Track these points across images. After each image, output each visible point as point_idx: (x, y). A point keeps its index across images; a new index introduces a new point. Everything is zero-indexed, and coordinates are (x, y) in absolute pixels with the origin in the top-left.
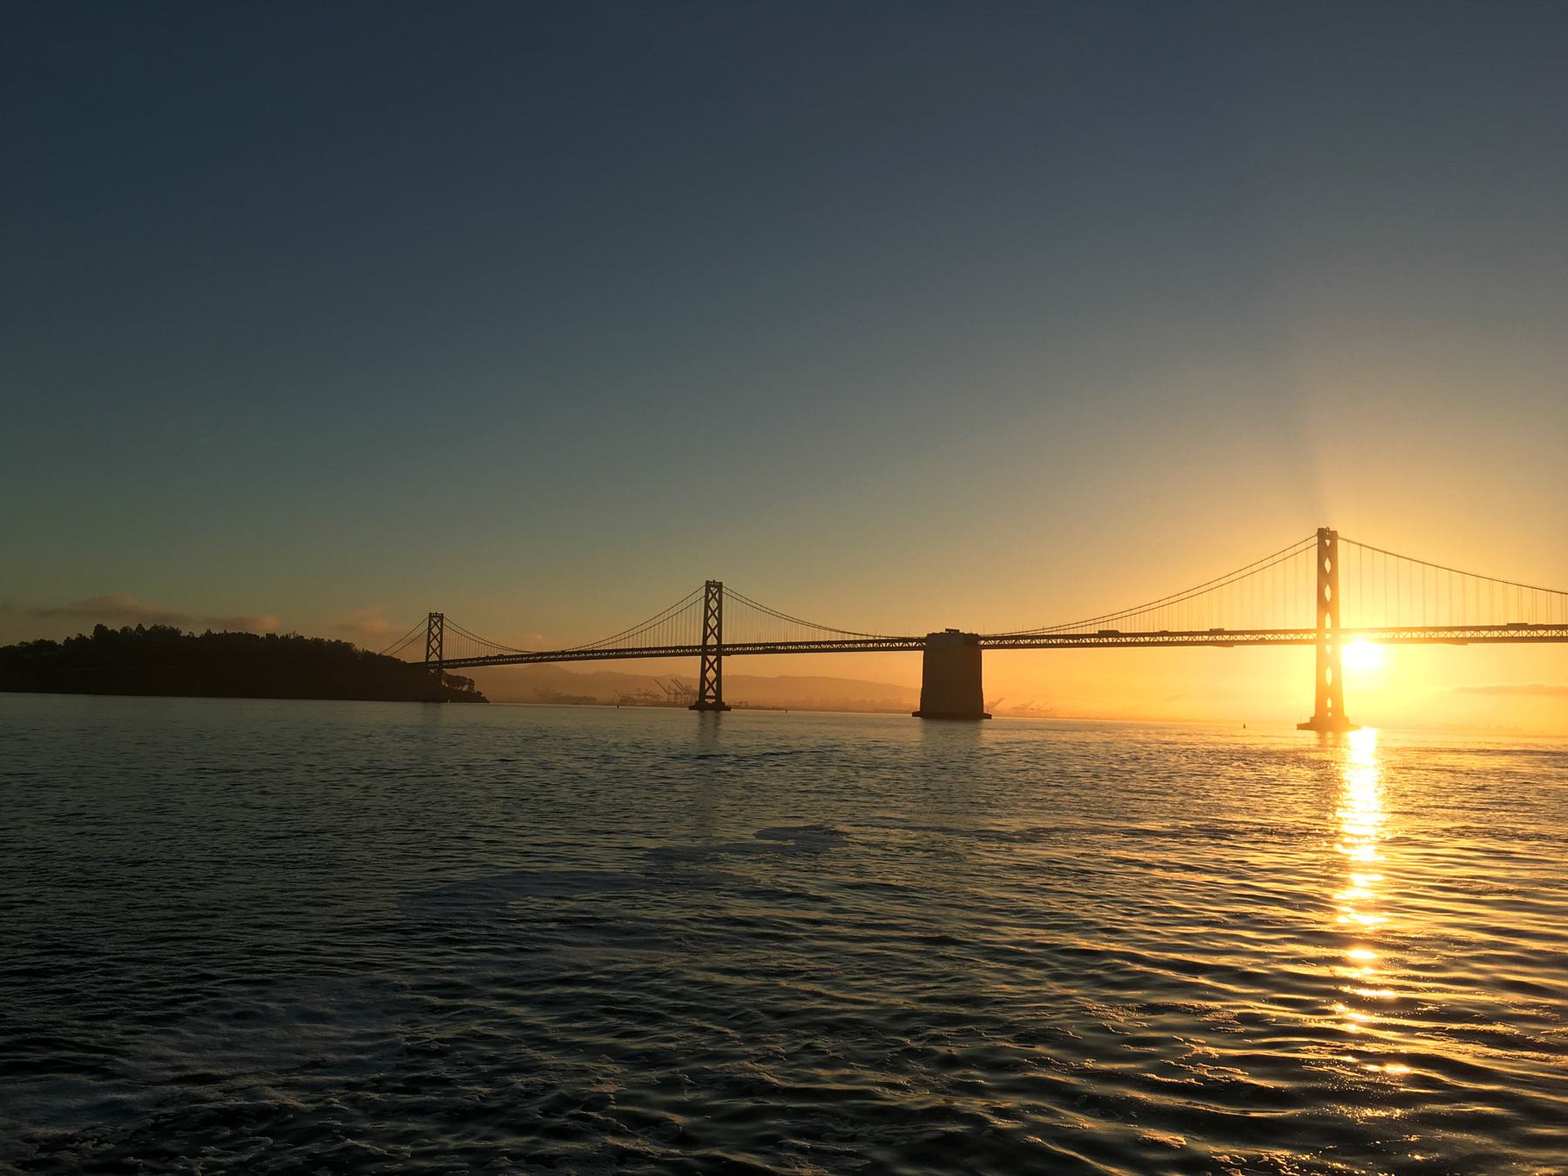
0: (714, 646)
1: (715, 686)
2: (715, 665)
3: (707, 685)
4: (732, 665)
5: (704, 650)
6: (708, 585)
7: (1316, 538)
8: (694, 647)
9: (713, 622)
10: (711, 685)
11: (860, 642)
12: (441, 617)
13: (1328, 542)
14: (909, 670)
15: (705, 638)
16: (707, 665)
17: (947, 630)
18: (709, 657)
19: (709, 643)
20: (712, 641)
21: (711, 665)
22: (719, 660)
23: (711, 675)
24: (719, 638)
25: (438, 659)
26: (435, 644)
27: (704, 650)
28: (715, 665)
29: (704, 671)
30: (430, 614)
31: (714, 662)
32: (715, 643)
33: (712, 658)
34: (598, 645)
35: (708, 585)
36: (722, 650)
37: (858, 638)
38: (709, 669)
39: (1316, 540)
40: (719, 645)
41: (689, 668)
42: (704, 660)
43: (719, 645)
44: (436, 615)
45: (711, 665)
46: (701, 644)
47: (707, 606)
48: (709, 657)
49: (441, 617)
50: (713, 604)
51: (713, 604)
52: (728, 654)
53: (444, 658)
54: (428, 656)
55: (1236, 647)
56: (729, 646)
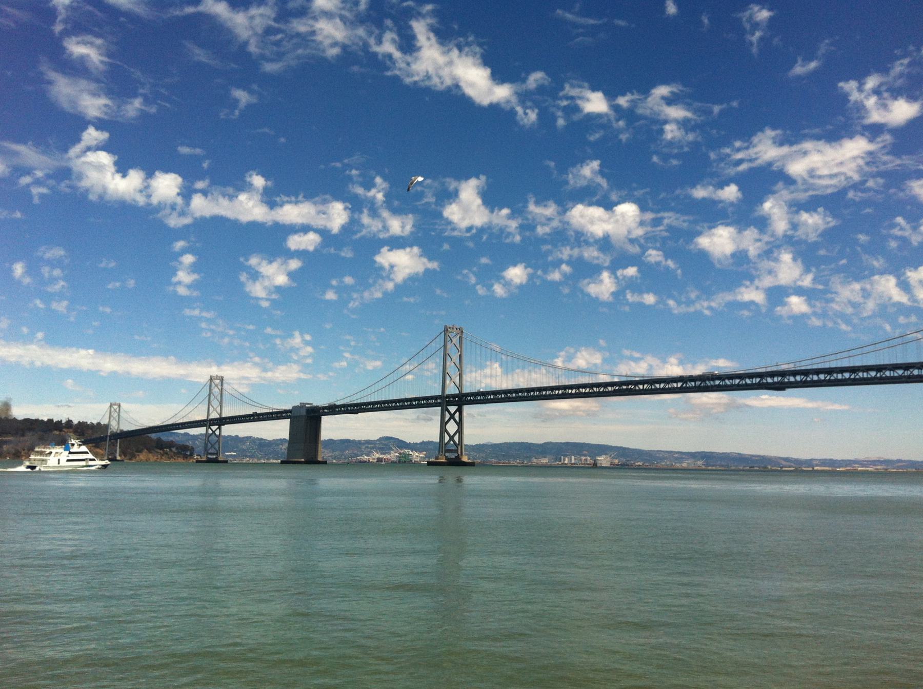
0: (454, 396)
2: (457, 416)
8: (435, 398)
10: (452, 438)
16: (447, 416)
18: (448, 407)
19: (448, 392)
20: (451, 390)
22: (460, 410)
23: (452, 427)
25: (217, 416)
26: (215, 403)
28: (457, 416)
30: (211, 377)
31: (455, 413)
33: (453, 409)
35: (446, 330)
36: (462, 400)
44: (217, 377)
45: (452, 416)
47: (445, 355)
48: (448, 407)
53: (225, 414)
54: (208, 415)
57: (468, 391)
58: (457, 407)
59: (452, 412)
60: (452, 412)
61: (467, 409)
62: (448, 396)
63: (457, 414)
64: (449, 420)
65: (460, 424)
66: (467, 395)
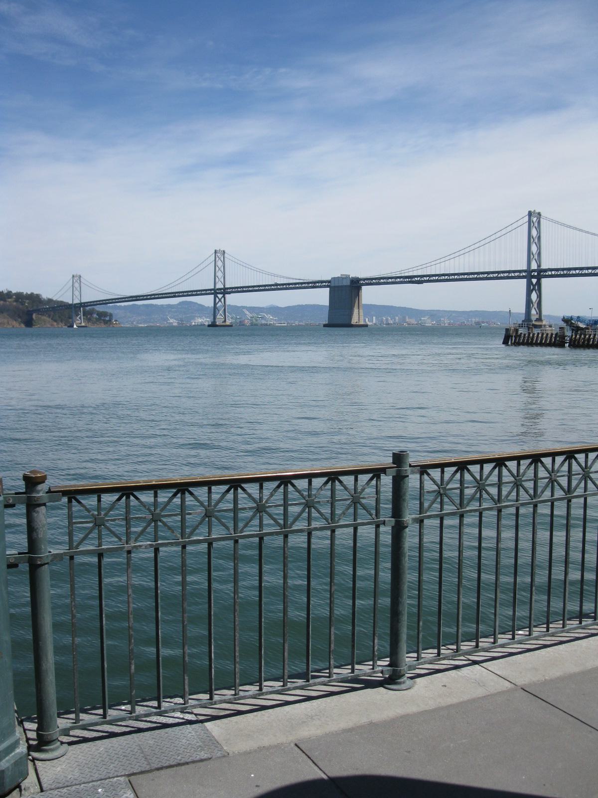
0: (220, 289)
4: (232, 299)
7: (527, 216)
9: (220, 274)
11: (298, 283)
13: (535, 219)
14: (322, 297)
16: (217, 300)
17: (341, 275)
18: (218, 295)
20: (220, 286)
21: (220, 300)
22: (224, 297)
27: (215, 292)
28: (223, 300)
29: (215, 304)
31: (221, 298)
33: (220, 296)
34: (164, 289)
35: (216, 252)
36: (225, 291)
37: (298, 281)
38: (219, 302)
39: (527, 219)
41: (207, 301)
45: (220, 300)
50: (220, 264)
51: (220, 264)
52: (229, 293)
55: (425, 284)
56: (230, 288)
57: (228, 286)
59: (220, 298)
60: (220, 298)
61: (227, 296)
62: (218, 289)
63: (223, 298)
64: (219, 302)
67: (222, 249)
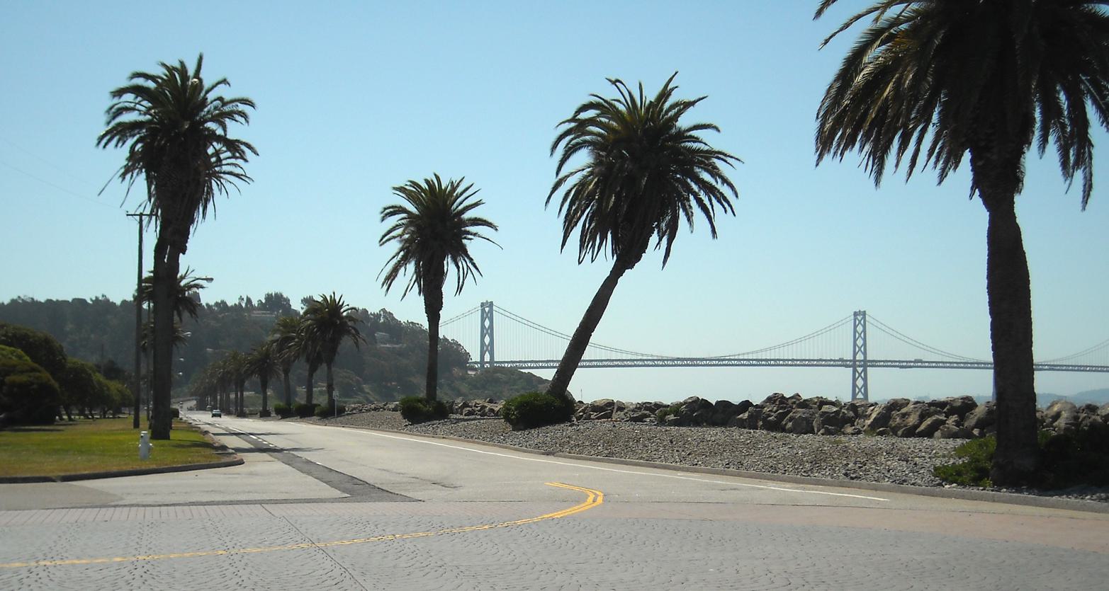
0: (860, 361)
1: (863, 390)
3: (857, 390)
5: (853, 364)
6: (856, 314)
12: (864, 314)
15: (855, 354)
21: (860, 375)
22: (865, 371)
23: (860, 383)
24: (865, 354)
27: (853, 364)
29: (855, 380)
32: (862, 358)
33: (860, 369)
35: (856, 314)
36: (866, 364)
40: (865, 361)
42: (855, 371)
43: (865, 361)
45: (860, 375)
46: (852, 359)
49: (864, 314)
58: (862, 368)
59: (860, 372)
60: (860, 372)
65: (865, 380)
66: (869, 361)
67: (862, 310)
